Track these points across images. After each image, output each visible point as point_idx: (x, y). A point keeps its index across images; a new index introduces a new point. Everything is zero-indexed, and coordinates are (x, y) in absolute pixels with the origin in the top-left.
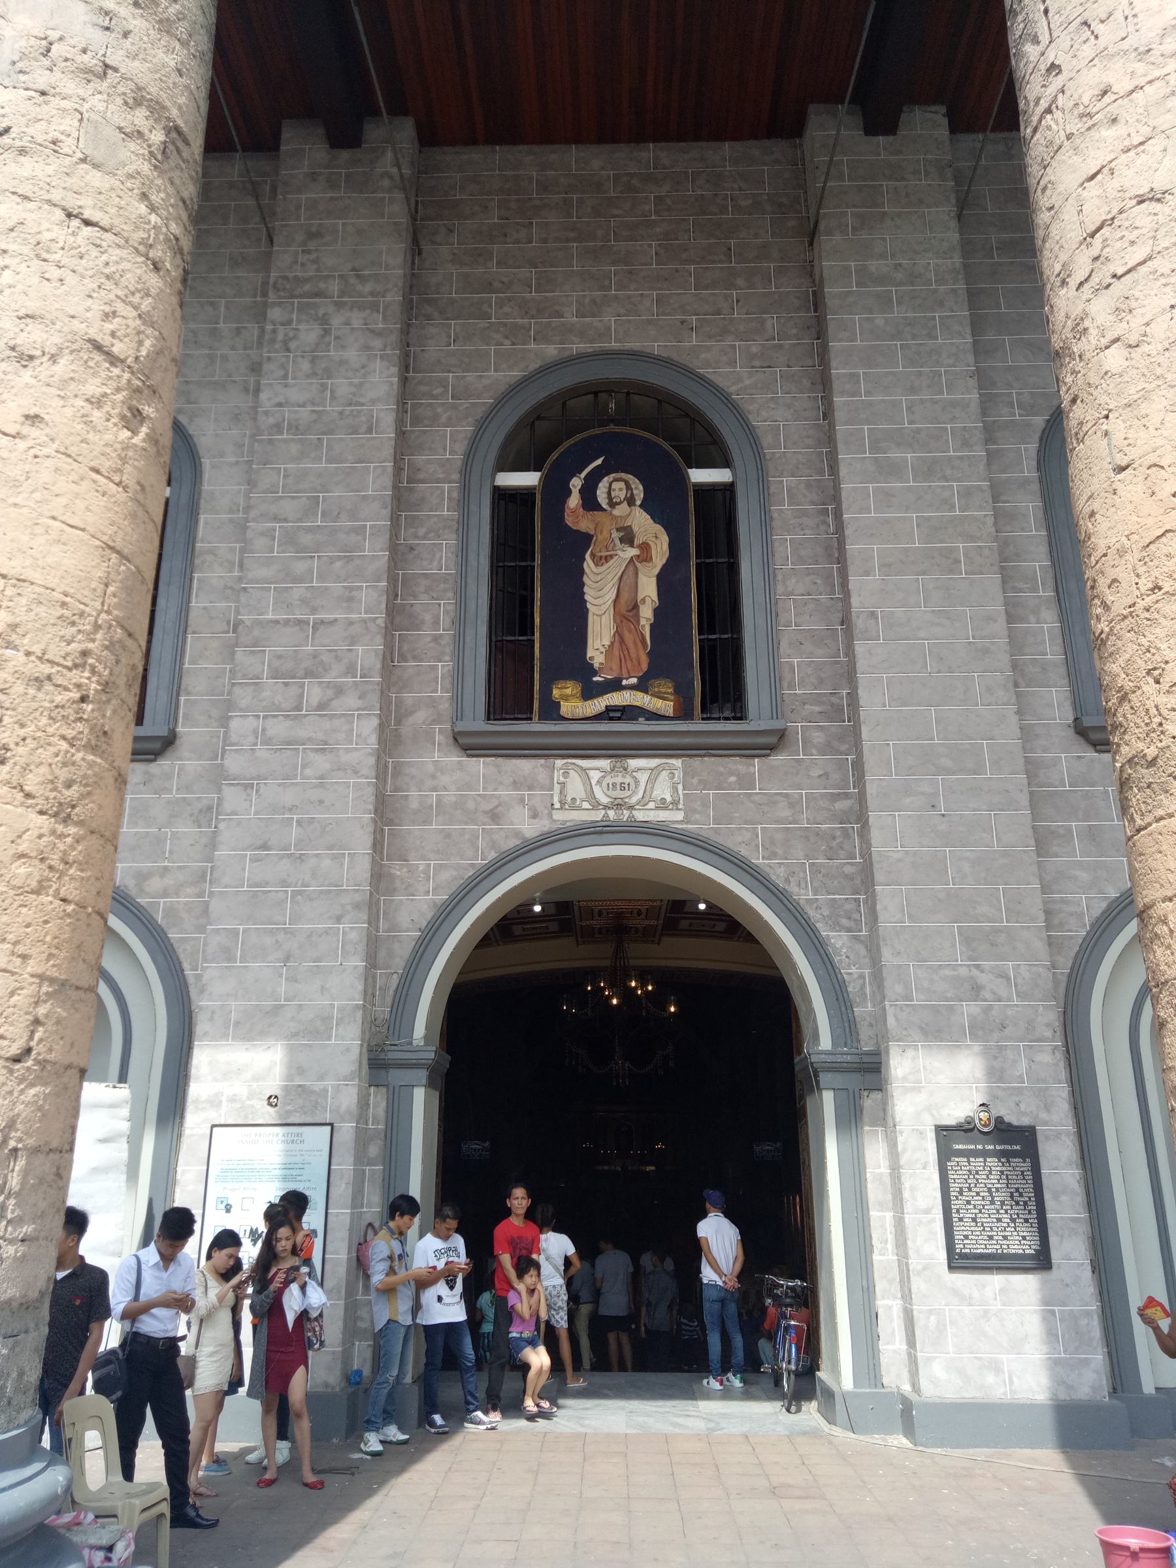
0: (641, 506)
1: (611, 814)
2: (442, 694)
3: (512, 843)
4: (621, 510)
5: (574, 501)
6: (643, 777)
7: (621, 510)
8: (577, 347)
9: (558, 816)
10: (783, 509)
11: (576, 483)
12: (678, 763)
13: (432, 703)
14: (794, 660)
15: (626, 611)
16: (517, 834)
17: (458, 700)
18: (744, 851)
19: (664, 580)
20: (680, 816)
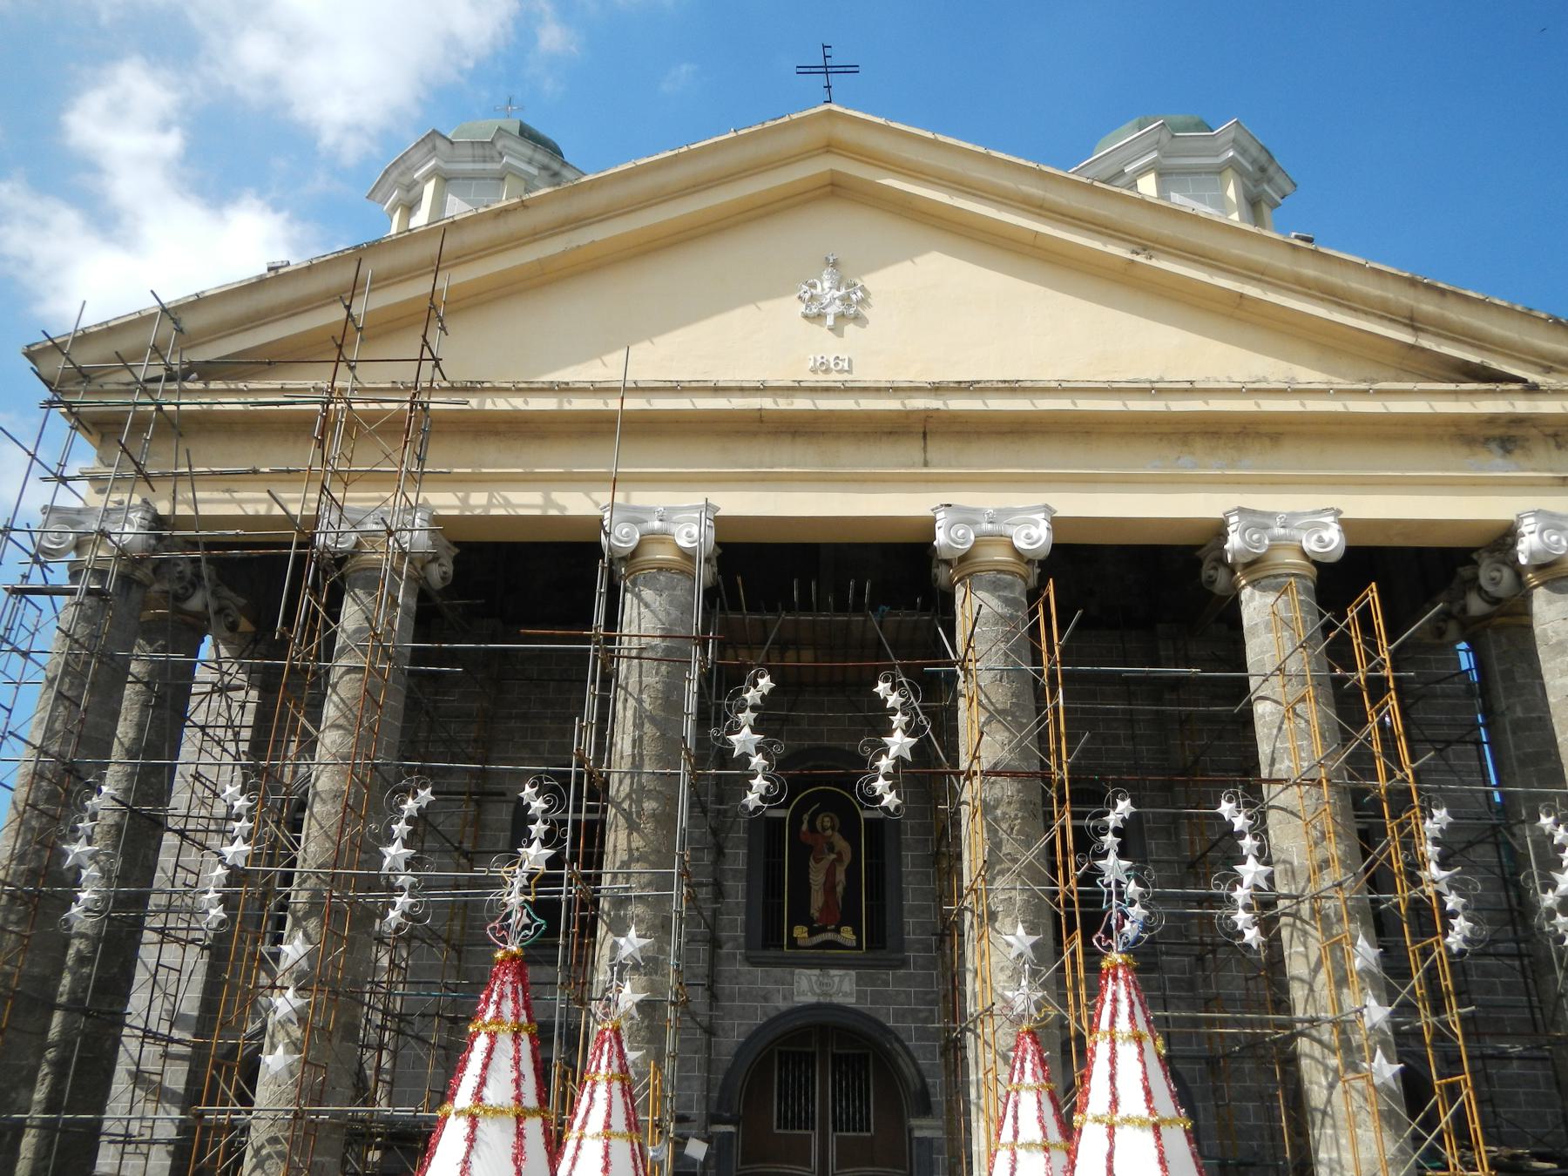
0: (840, 831)
1: (822, 1000)
2: (740, 933)
3: (773, 1014)
4: (829, 832)
5: (805, 827)
6: (837, 980)
7: (829, 832)
8: (807, 743)
9: (796, 999)
10: (907, 837)
11: (806, 817)
12: (853, 973)
13: (735, 939)
14: (910, 921)
15: (829, 887)
16: (777, 1008)
17: (748, 938)
18: (882, 1019)
19: (848, 872)
20: (854, 1000)
